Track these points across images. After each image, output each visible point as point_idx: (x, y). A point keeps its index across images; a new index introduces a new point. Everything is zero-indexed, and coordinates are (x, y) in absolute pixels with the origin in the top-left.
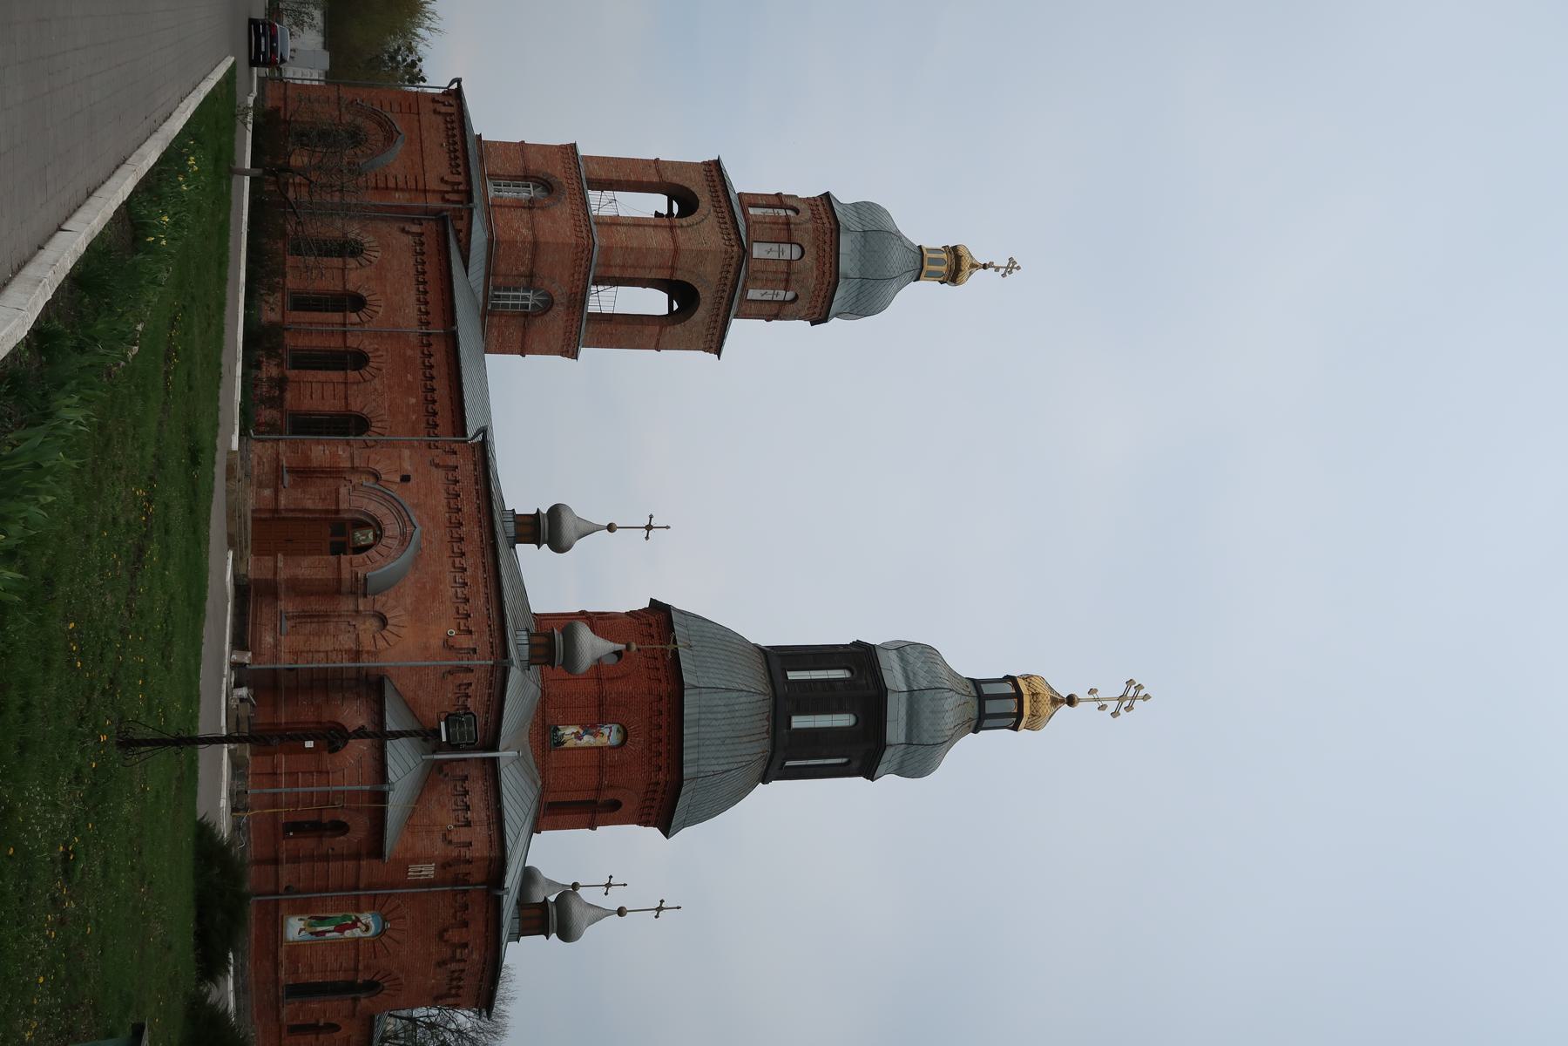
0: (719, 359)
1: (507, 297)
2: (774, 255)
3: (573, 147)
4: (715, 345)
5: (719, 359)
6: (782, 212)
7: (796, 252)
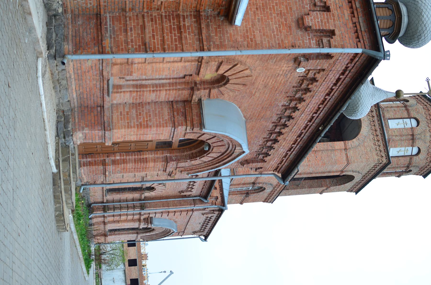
0: (356, 194)
2: (402, 154)
5: (356, 194)
7: (415, 150)
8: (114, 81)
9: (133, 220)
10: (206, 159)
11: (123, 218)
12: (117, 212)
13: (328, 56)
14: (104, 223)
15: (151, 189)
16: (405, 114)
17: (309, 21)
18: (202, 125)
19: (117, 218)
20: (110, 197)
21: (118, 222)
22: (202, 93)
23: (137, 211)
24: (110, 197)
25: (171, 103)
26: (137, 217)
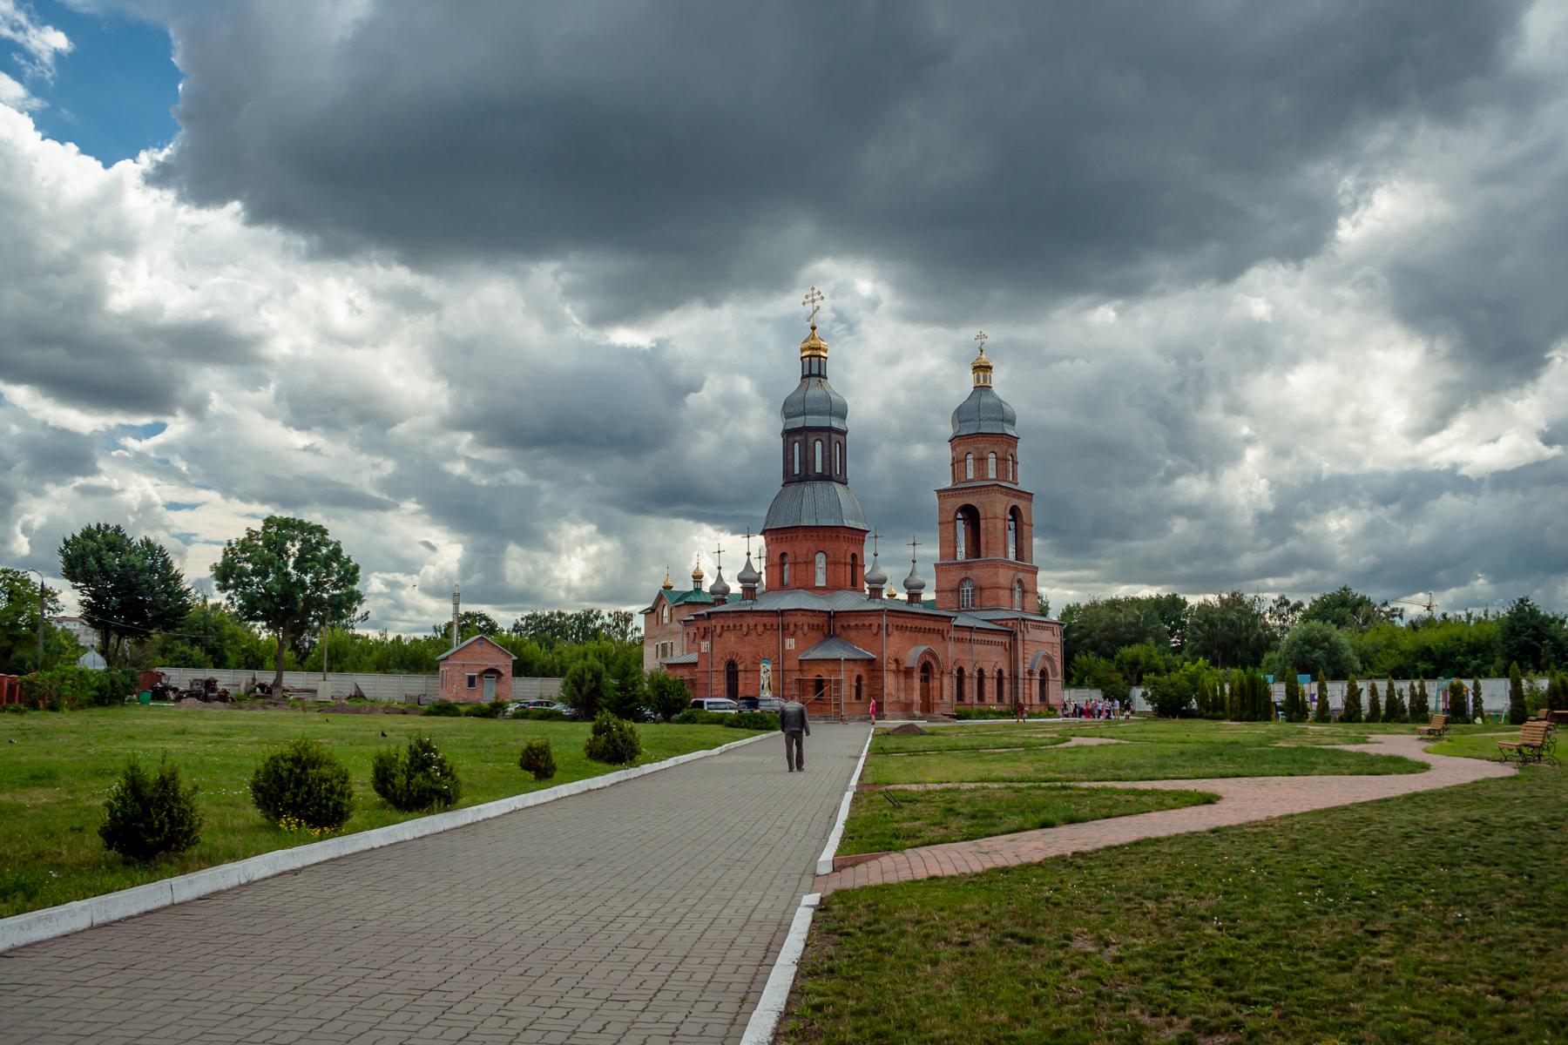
1: (968, 601)
3: (936, 566)
4: (1028, 496)
6: (970, 461)
7: (994, 456)
8: (895, 699)
9: (1030, 685)
10: (933, 662)
11: (1027, 691)
12: (1020, 696)
13: (887, 625)
14: (1031, 705)
15: (1000, 672)
16: (963, 464)
17: (875, 632)
18: (913, 668)
19: (1027, 696)
20: (1007, 701)
21: (1031, 695)
22: (902, 668)
23: (1020, 681)
24: (1007, 701)
25: (906, 678)
26: (1027, 681)
